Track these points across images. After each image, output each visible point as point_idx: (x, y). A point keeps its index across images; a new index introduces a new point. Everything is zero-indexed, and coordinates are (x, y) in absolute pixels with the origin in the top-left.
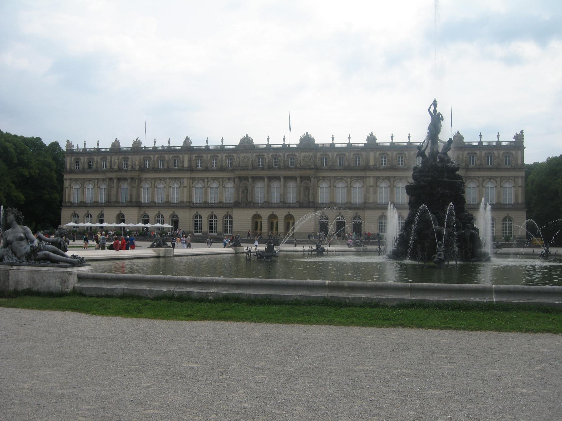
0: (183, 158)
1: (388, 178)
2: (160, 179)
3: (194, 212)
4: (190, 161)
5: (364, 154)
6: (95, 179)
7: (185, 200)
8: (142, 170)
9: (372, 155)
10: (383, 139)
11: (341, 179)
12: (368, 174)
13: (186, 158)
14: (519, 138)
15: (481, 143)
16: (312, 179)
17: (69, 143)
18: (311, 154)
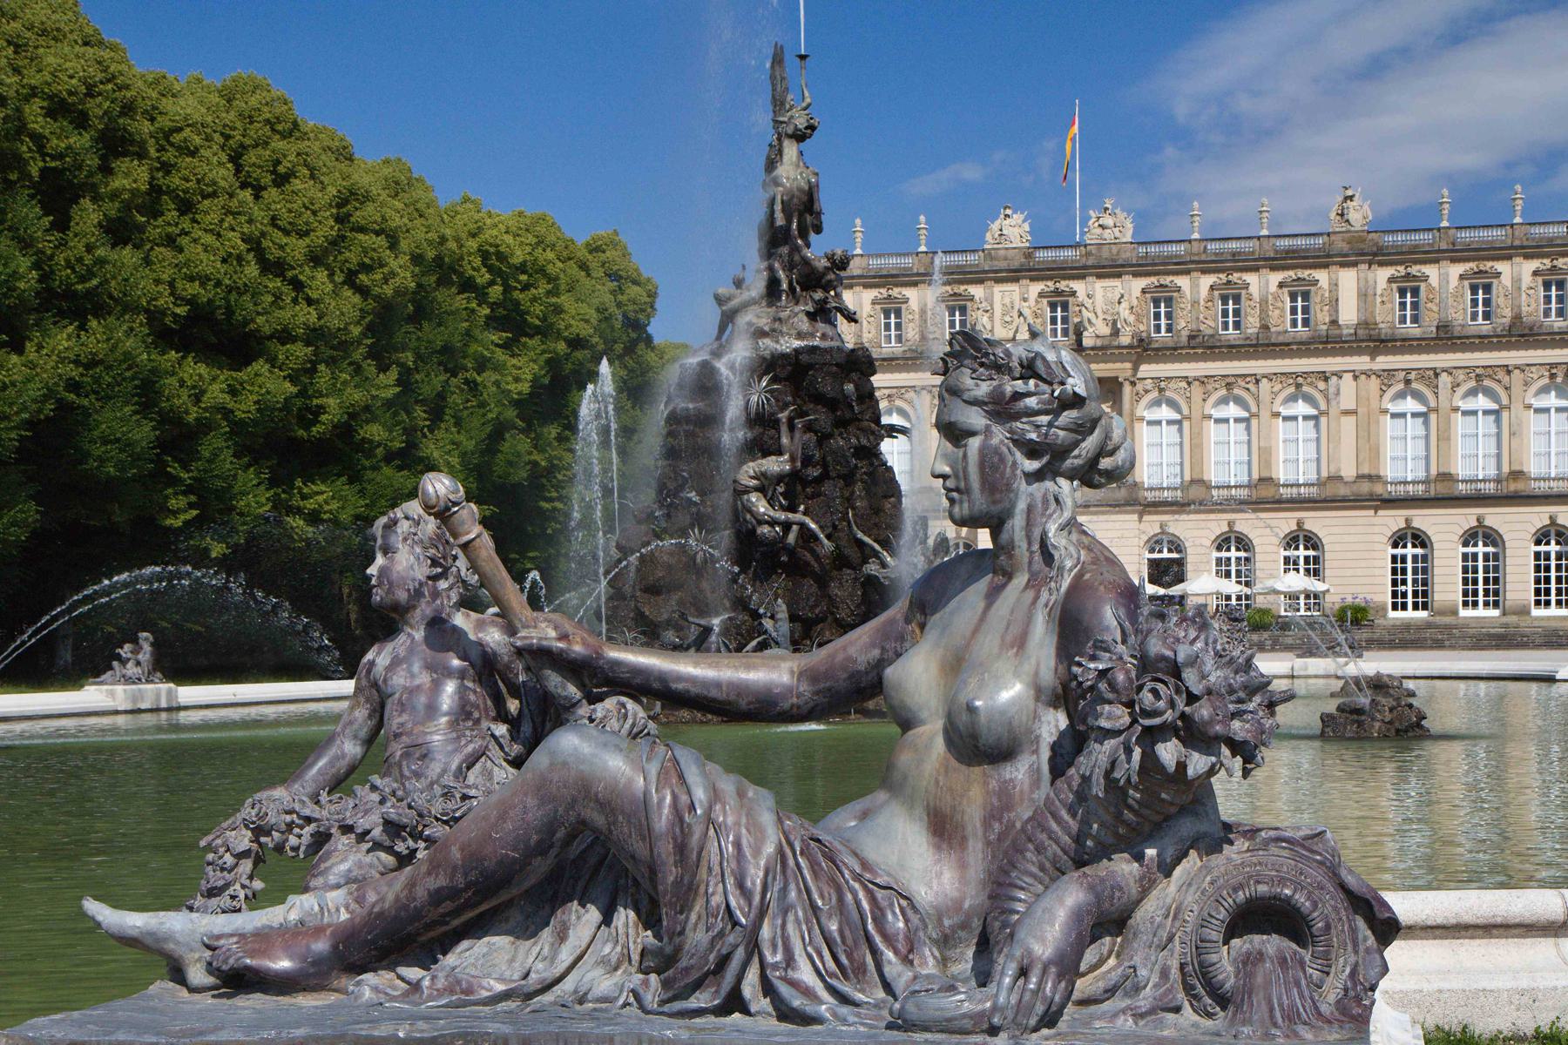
0: (1335, 285)
2: (1229, 382)
3: (1393, 520)
4: (1364, 295)
7: (1349, 472)
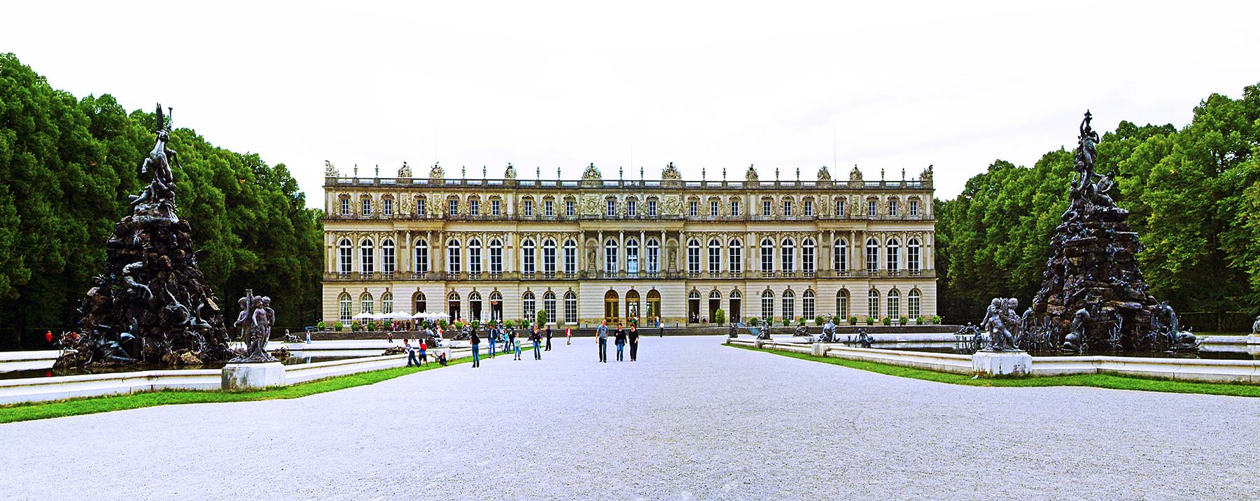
6: (374, 232)
8: (447, 219)
12: (750, 228)
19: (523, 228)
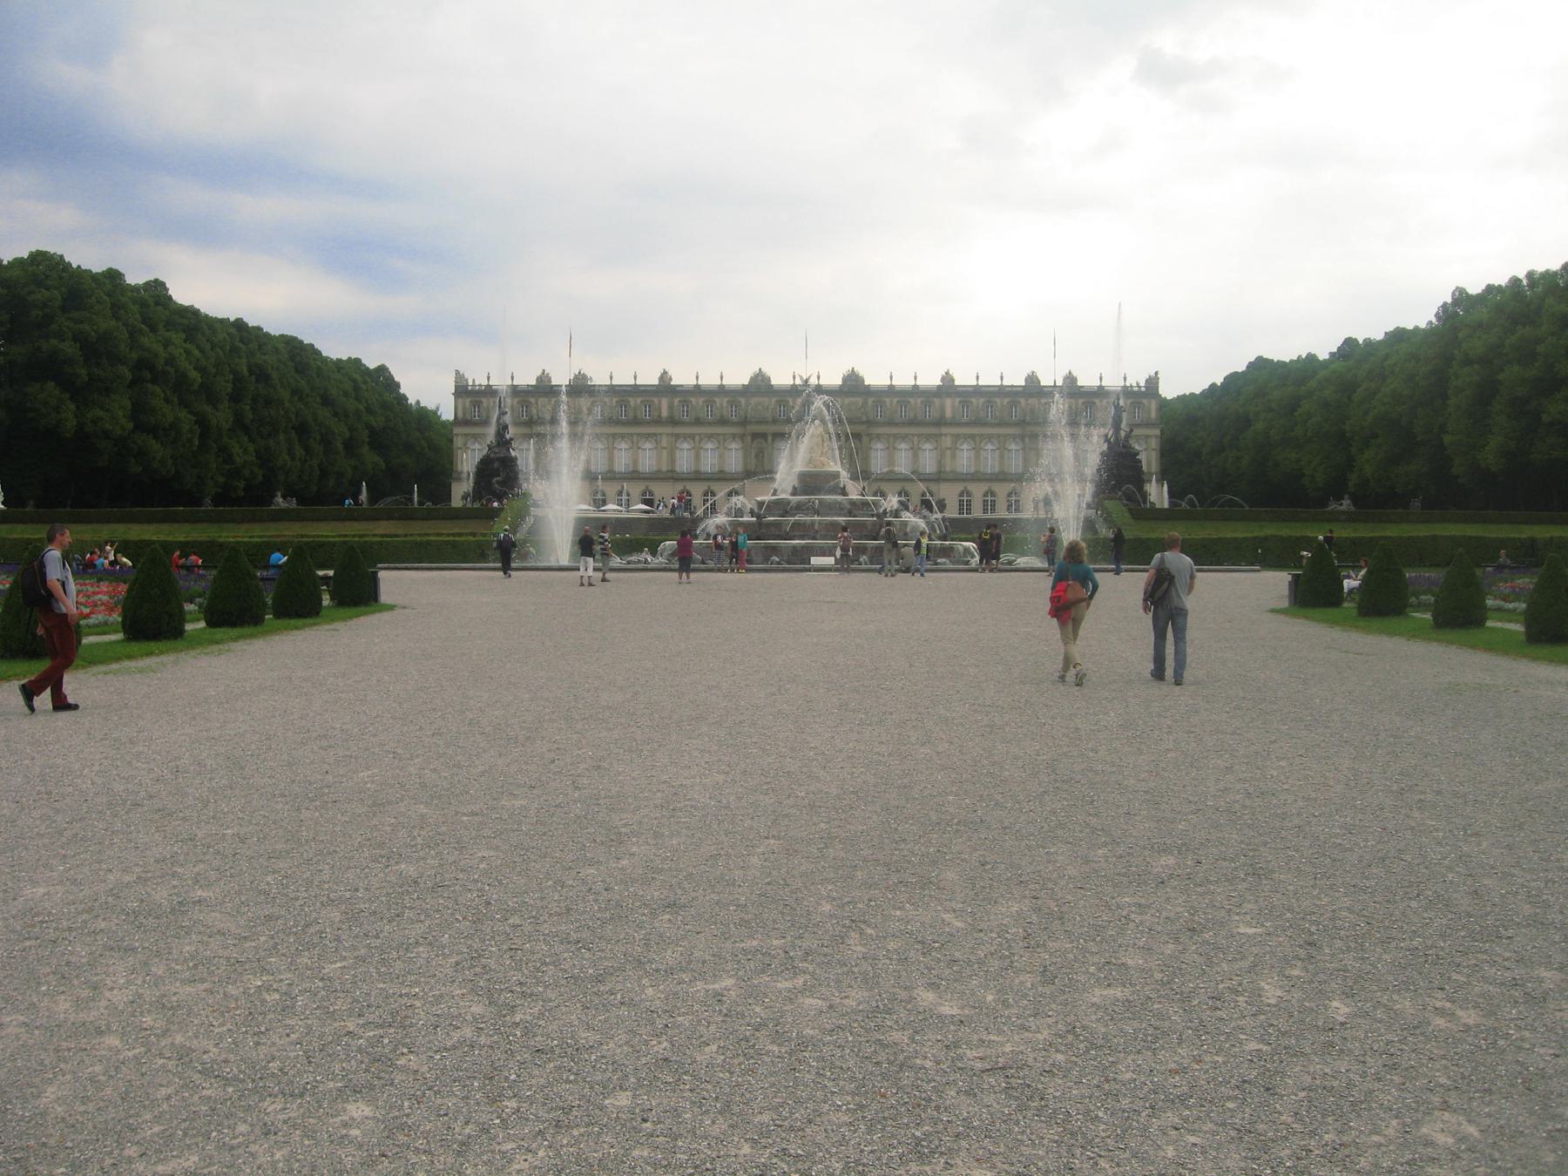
1: (972, 437)
3: (679, 487)
4: (671, 407)
5: (936, 401)
7: (664, 469)
9: (948, 402)
10: (963, 379)
11: (904, 438)
12: (945, 430)
13: (665, 402)
14: (1153, 382)
15: (1101, 387)
16: (865, 438)
17: (459, 376)
18: (860, 400)
19: (678, 430)
